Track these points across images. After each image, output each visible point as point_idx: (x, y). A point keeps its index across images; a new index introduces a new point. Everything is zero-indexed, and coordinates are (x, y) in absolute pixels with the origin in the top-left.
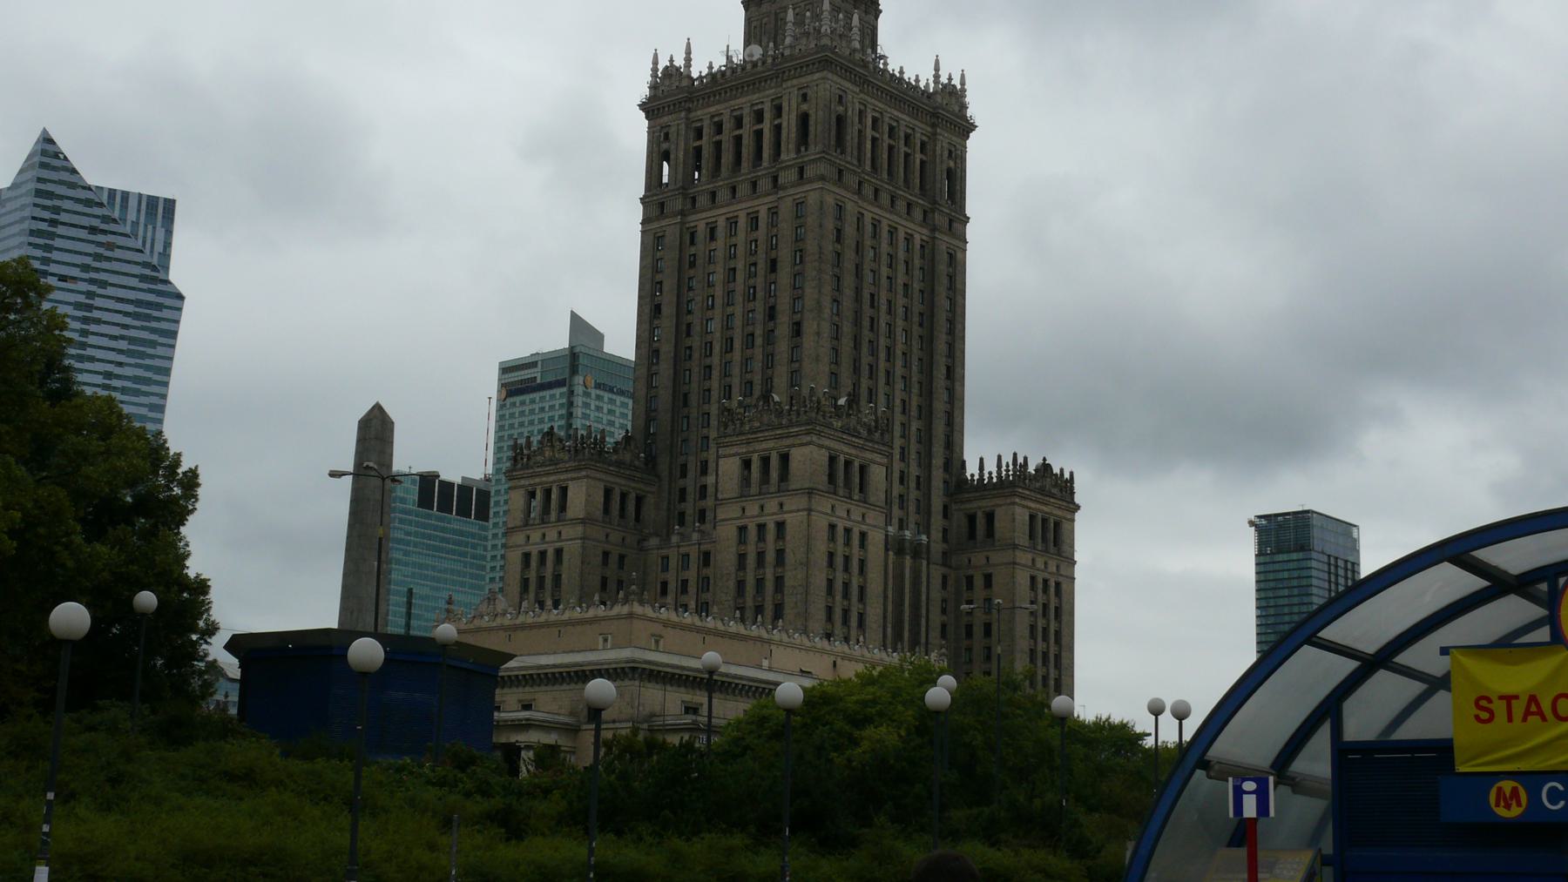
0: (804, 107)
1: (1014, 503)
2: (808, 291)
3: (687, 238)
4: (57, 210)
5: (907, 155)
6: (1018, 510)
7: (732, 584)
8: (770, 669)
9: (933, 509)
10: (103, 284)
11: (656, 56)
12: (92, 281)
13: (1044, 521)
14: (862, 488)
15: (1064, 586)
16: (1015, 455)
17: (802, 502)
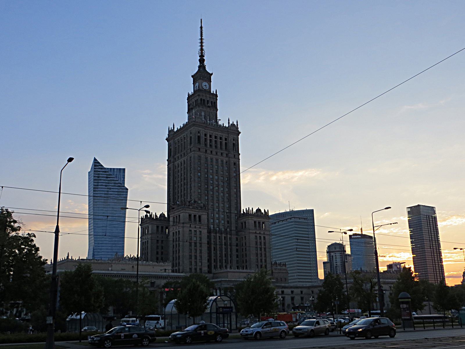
0: (191, 135)
1: (249, 219)
2: (192, 176)
3: (175, 167)
4: (99, 174)
5: (220, 142)
6: (250, 221)
7: (172, 246)
8: (112, 270)
9: (232, 223)
10: (110, 189)
11: (169, 128)
12: (108, 188)
13: (259, 223)
14: (200, 221)
15: (267, 237)
16: (249, 208)
17: (182, 225)
